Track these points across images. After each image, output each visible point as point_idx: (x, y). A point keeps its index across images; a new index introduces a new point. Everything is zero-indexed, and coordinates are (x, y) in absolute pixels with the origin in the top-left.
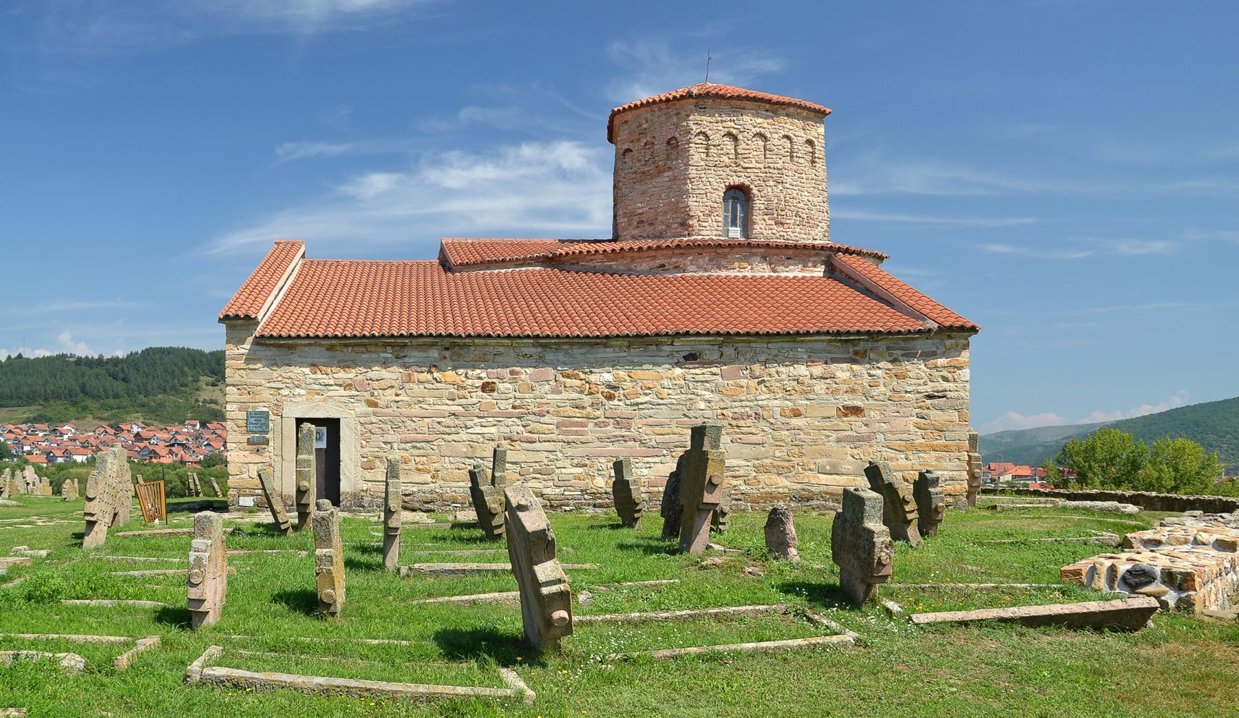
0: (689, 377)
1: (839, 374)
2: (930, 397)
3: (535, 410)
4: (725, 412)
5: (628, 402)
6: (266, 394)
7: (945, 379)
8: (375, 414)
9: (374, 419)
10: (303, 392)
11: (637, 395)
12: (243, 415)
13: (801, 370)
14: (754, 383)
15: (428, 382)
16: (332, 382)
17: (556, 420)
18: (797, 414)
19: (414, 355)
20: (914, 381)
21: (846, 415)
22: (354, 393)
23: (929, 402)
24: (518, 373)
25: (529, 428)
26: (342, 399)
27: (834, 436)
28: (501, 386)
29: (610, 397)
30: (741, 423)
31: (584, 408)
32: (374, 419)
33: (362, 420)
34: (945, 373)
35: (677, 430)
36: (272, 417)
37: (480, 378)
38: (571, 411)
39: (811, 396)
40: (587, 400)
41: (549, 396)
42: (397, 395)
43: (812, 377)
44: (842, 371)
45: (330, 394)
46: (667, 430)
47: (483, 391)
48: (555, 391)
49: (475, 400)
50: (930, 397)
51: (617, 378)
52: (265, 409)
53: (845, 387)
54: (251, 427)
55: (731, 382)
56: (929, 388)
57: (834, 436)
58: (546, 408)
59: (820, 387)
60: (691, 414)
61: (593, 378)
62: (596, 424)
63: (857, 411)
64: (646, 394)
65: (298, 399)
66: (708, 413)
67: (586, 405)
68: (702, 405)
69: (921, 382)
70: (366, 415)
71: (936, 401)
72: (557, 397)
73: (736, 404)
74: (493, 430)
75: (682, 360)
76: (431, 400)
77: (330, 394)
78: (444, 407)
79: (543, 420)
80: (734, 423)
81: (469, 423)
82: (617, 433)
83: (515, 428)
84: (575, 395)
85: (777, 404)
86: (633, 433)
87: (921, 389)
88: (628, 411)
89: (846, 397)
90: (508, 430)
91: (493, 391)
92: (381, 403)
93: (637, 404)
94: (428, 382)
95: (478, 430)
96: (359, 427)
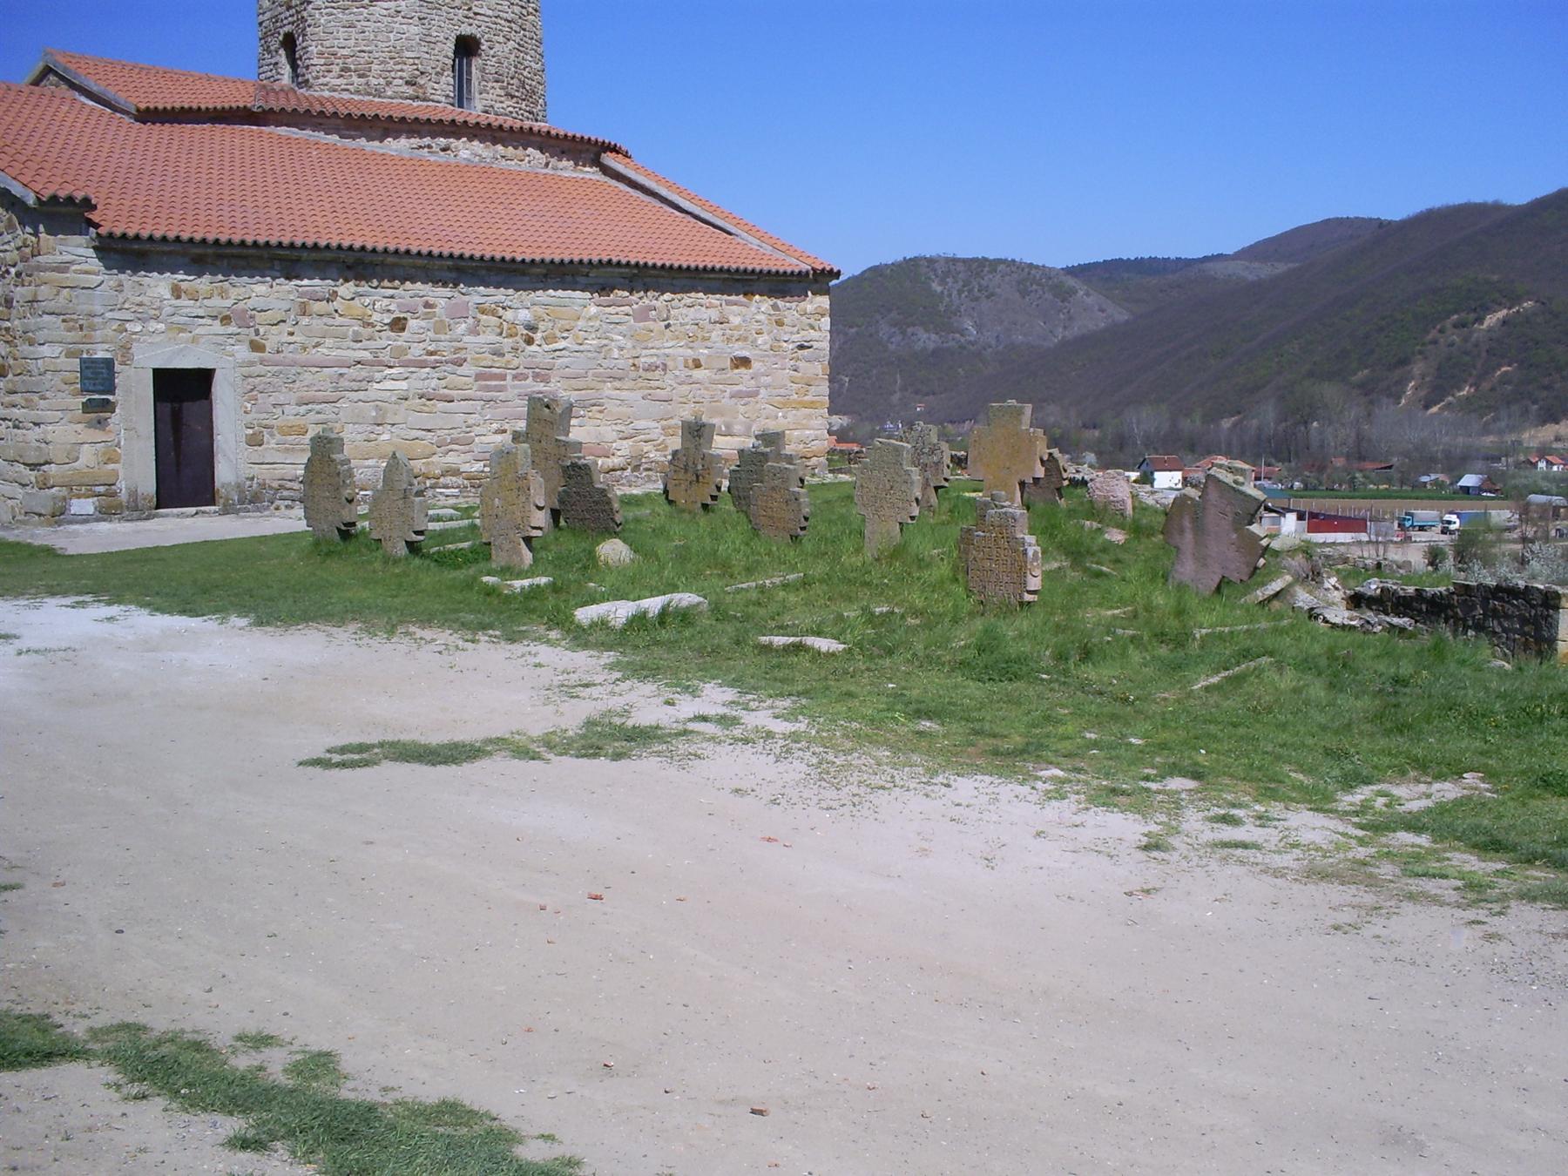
1: (731, 318)
5: (546, 348)
9: (260, 369)
10: (161, 326)
11: (554, 339)
12: (75, 363)
15: (329, 315)
18: (697, 365)
26: (220, 339)
29: (530, 341)
30: (649, 375)
32: (260, 369)
33: (245, 371)
34: (812, 321)
38: (489, 359)
41: (466, 339)
42: (292, 334)
45: (199, 331)
46: (580, 383)
48: (474, 331)
49: (384, 343)
50: (801, 347)
52: (108, 356)
57: (729, 389)
58: (461, 355)
59: (716, 334)
60: (605, 363)
62: (515, 377)
63: (744, 362)
65: (158, 339)
68: (616, 353)
70: (251, 364)
71: (806, 352)
74: (404, 385)
77: (199, 331)
79: (460, 370)
81: (378, 376)
90: (420, 384)
91: (403, 329)
94: (329, 315)
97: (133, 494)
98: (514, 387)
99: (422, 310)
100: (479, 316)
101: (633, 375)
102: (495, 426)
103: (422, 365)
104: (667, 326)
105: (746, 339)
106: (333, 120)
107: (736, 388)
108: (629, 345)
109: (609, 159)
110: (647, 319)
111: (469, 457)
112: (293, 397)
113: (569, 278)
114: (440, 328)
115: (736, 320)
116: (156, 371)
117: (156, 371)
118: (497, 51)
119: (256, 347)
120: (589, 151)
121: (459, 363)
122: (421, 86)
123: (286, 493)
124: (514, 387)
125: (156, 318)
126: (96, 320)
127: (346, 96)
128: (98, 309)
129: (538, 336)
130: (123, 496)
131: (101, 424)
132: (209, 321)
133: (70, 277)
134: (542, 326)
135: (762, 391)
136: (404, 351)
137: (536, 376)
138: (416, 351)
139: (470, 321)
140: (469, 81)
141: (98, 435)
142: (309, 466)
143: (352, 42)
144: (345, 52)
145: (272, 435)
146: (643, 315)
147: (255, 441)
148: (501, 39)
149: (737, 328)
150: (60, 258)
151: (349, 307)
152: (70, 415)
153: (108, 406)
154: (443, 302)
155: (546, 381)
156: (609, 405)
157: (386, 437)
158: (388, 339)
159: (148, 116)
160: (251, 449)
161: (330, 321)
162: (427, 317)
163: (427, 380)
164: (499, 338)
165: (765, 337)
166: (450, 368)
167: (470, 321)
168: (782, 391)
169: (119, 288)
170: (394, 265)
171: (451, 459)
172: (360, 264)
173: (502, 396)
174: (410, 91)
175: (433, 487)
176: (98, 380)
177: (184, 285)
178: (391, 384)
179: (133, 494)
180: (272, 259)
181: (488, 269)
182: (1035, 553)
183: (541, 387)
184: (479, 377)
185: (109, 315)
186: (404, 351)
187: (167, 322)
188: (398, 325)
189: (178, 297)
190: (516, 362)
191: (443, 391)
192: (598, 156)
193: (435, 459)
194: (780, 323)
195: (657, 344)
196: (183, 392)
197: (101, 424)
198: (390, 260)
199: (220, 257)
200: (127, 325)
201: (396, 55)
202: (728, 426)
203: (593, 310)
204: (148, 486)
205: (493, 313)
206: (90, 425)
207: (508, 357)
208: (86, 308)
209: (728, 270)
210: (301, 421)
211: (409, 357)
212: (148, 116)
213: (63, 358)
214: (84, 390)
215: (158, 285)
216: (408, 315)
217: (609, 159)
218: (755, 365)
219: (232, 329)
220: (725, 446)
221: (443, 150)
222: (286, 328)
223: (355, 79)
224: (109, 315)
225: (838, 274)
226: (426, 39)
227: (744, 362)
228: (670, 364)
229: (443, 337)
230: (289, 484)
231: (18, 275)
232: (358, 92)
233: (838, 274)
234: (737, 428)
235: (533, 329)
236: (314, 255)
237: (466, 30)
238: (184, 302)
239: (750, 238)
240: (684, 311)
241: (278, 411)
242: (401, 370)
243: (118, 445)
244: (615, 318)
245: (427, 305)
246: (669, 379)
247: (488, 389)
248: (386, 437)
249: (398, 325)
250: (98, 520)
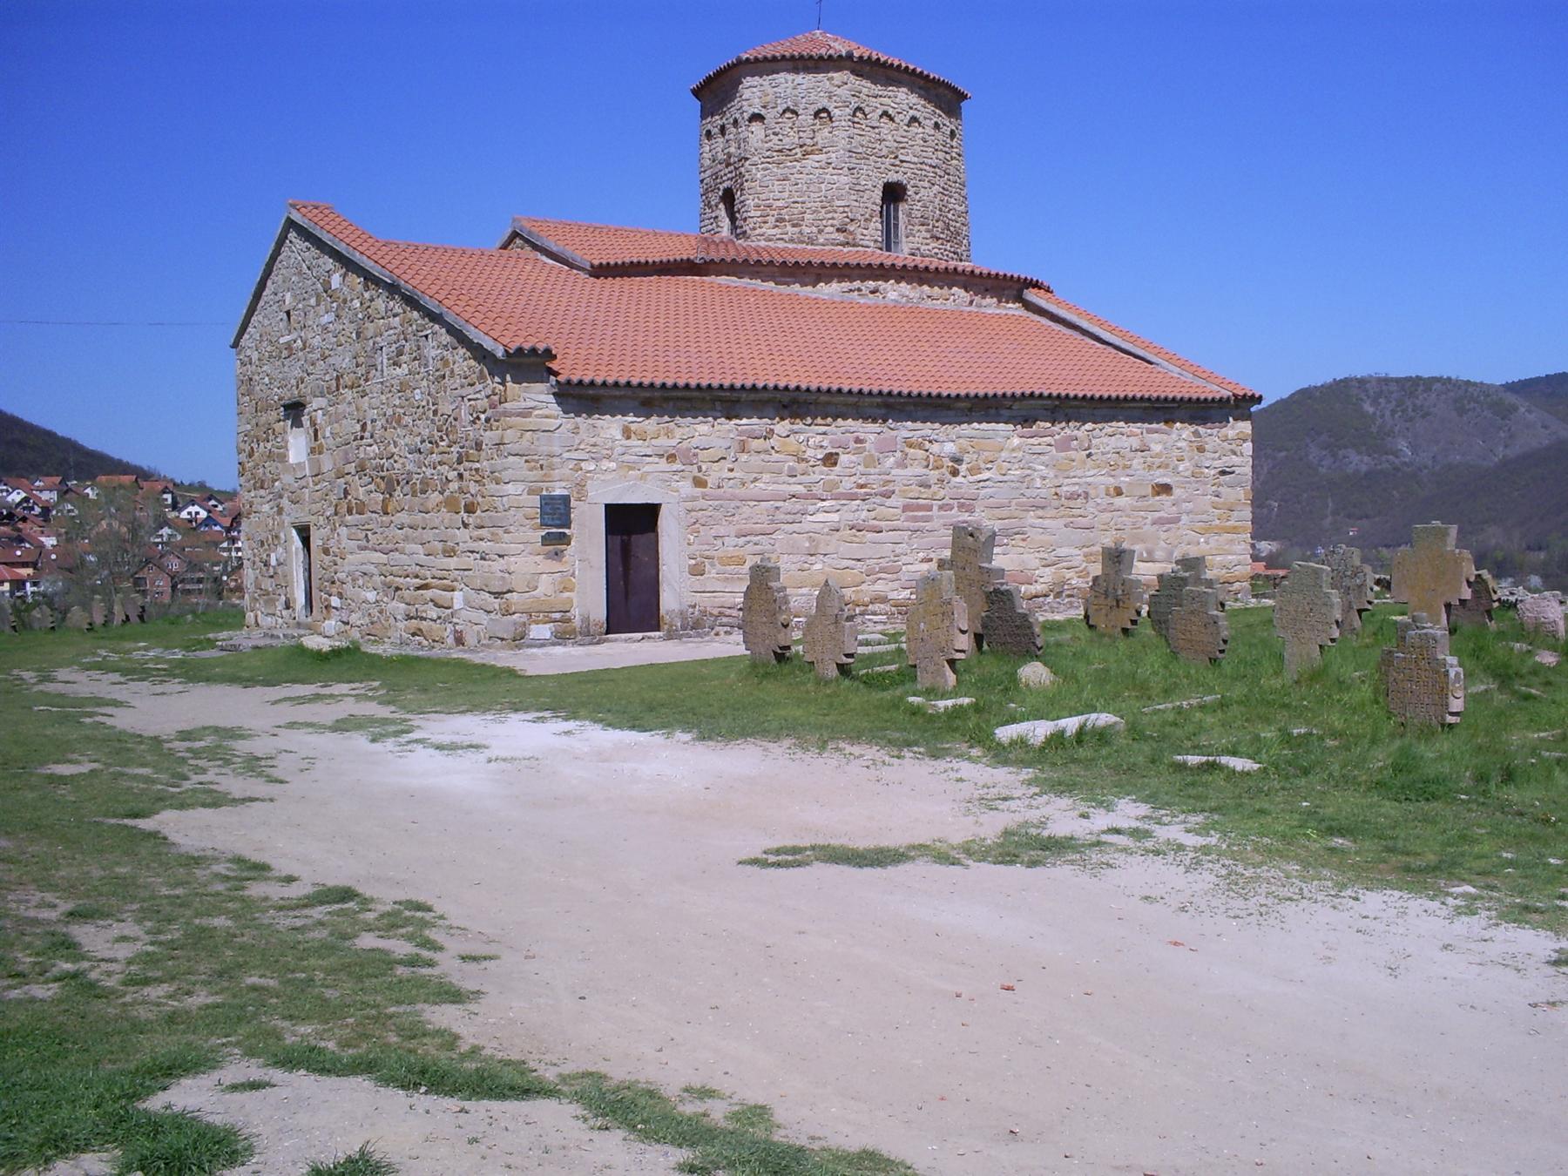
5: (971, 478)
9: (702, 503)
10: (613, 465)
11: (979, 470)
15: (766, 452)
18: (1119, 492)
19: (571, 400)
29: (955, 473)
30: (1071, 503)
32: (702, 503)
33: (689, 505)
34: (1233, 447)
35: (1016, 513)
38: (915, 490)
41: (894, 472)
42: (731, 470)
45: (647, 468)
46: (1004, 513)
48: (901, 464)
49: (817, 477)
50: (1223, 473)
52: (566, 493)
53: (1157, 461)
57: (1151, 516)
58: (890, 487)
59: (1137, 462)
60: (1028, 492)
62: (941, 508)
63: (1165, 489)
65: (609, 477)
68: (1038, 483)
70: (694, 499)
71: (1227, 477)
74: (835, 517)
77: (647, 468)
79: (888, 502)
81: (811, 509)
89: (1158, 472)
90: (851, 516)
91: (835, 464)
94: (766, 452)
97: (586, 620)
99: (852, 445)
100: (907, 450)
101: (1056, 503)
102: (921, 555)
103: (853, 497)
104: (1089, 455)
105: (1167, 466)
106: (770, 268)
107: (1157, 515)
108: (1052, 475)
109: (1031, 295)
110: (1068, 449)
111: (896, 585)
112: (733, 530)
113: (993, 411)
114: (871, 462)
115: (1157, 448)
116: (607, 506)
117: (607, 506)
118: (922, 197)
119: (699, 483)
120: (1012, 288)
121: (888, 495)
122: (851, 233)
123: (725, 620)
125: (608, 457)
126: (555, 460)
127: (781, 245)
128: (556, 450)
129: (963, 468)
130: (577, 623)
131: (557, 555)
133: (531, 422)
134: (966, 458)
135: (1184, 517)
136: (836, 485)
137: (961, 506)
138: (847, 485)
139: (898, 454)
140: (896, 226)
141: (554, 566)
142: (748, 594)
143: (786, 195)
144: (780, 204)
145: (713, 565)
146: (1064, 446)
147: (697, 571)
148: (926, 184)
149: (1158, 455)
150: (523, 405)
151: (785, 444)
152: (530, 547)
153: (564, 539)
154: (872, 437)
155: (971, 511)
156: (1031, 533)
157: (818, 566)
158: (821, 474)
159: (601, 271)
162: (858, 452)
163: (858, 512)
164: (925, 471)
165: (1187, 464)
166: (878, 500)
167: (898, 454)
168: (1204, 517)
169: (576, 430)
170: (828, 403)
171: (880, 587)
172: (794, 403)
173: (928, 526)
174: (841, 237)
175: (862, 614)
176: (556, 515)
177: (633, 427)
178: (823, 516)
179: (586, 620)
181: (915, 405)
182: (1457, 674)
183: (965, 517)
184: (906, 508)
185: (566, 455)
186: (836, 485)
187: (618, 461)
188: (830, 460)
189: (628, 438)
190: (942, 493)
192: (1020, 292)
193: (864, 587)
194: (1201, 450)
195: (1079, 473)
196: (632, 525)
197: (557, 555)
198: (823, 398)
199: (667, 399)
200: (582, 464)
201: (827, 204)
202: (1150, 553)
203: (1016, 441)
204: (600, 613)
205: (920, 446)
206: (548, 556)
207: (935, 488)
208: (544, 449)
209: (1149, 399)
210: (740, 552)
211: (841, 490)
212: (601, 271)
213: (525, 496)
214: (544, 524)
215: (610, 427)
216: (839, 450)
217: (1031, 295)
218: (1177, 492)
219: (677, 466)
220: (1145, 572)
221: (872, 292)
222: (727, 464)
223: (789, 228)
224: (566, 455)
225: (1260, 399)
226: (856, 188)
227: (1165, 489)
228: (1092, 493)
229: (872, 471)
230: (728, 612)
231: (488, 420)
232: (792, 241)
233: (1260, 399)
234: (1159, 554)
235: (958, 460)
236: (752, 396)
237: (893, 177)
238: (634, 442)
239: (1171, 367)
240: (1105, 440)
241: (719, 542)
243: (573, 575)
244: (1038, 449)
245: (858, 441)
246: (1090, 507)
247: (915, 519)
248: (818, 566)
249: (830, 460)
250: (554, 644)
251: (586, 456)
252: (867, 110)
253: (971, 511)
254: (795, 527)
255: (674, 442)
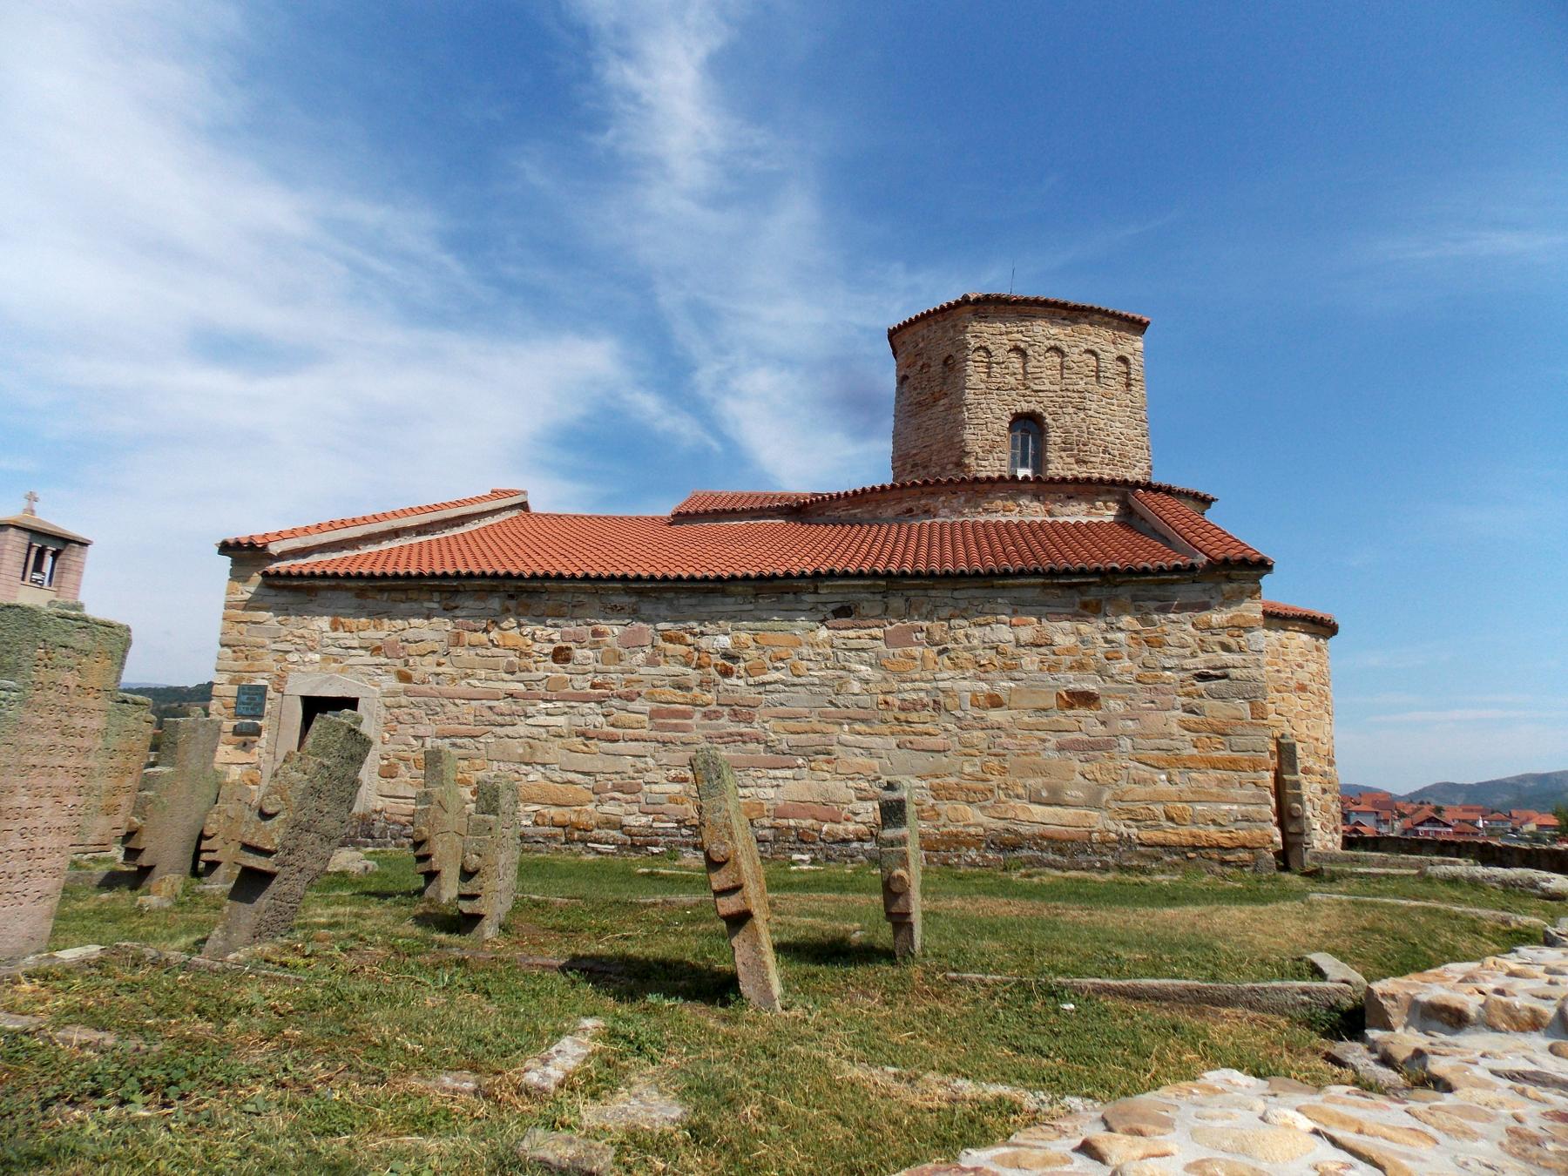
0: (837, 642)
2: (1203, 677)
3: (623, 690)
4: (889, 698)
5: (751, 681)
6: (268, 661)
7: (1226, 648)
8: (406, 692)
9: (404, 700)
10: (317, 657)
11: (763, 669)
13: (1003, 633)
14: (931, 652)
15: (482, 645)
16: (355, 643)
17: (648, 706)
18: (995, 702)
20: (1175, 651)
21: (1071, 707)
22: (383, 660)
23: (1201, 685)
24: (602, 634)
25: (611, 719)
27: (1053, 740)
28: (578, 654)
29: (726, 673)
30: (913, 716)
31: (689, 689)
32: (404, 700)
33: (388, 701)
34: (1225, 638)
35: (819, 727)
36: (271, 694)
37: (551, 641)
39: (1016, 675)
40: (693, 675)
41: (642, 670)
42: (439, 665)
43: (1018, 644)
44: (1063, 633)
46: (804, 726)
47: (555, 661)
48: (652, 662)
49: (541, 674)
50: (1203, 677)
51: (736, 643)
52: (265, 683)
54: (242, 709)
55: (898, 651)
56: (1200, 663)
57: (1053, 740)
58: (636, 688)
59: (1030, 660)
60: (840, 700)
61: (703, 643)
62: (705, 715)
63: (1087, 699)
64: (776, 669)
65: (310, 668)
66: (865, 700)
67: (693, 684)
68: (856, 687)
69: (1188, 652)
70: (394, 694)
71: (1213, 684)
72: (653, 671)
73: (908, 686)
74: (561, 720)
75: (829, 615)
76: (483, 673)
78: (499, 685)
79: (631, 706)
80: (902, 716)
81: (531, 710)
82: (733, 728)
83: (590, 719)
84: (678, 669)
85: (967, 685)
86: (756, 728)
87: (1189, 663)
88: (751, 694)
89: (1071, 675)
90: (581, 721)
91: (567, 660)
92: (416, 676)
93: (764, 684)
94: (482, 645)
95: (542, 720)
96: (383, 712)
98: (704, 727)
102: (673, 773)
103: (586, 699)
119: (405, 677)
124: (704, 727)
132: (362, 652)
138: (582, 684)
139: (648, 650)
141: (242, 756)
145: (408, 767)
148: (1071, 410)
155: (749, 721)
158: (549, 669)
160: (383, 781)
161: (484, 652)
162: (595, 646)
163: (592, 716)
166: (616, 702)
168: (1164, 743)
171: (609, 808)
178: (548, 717)
180: (432, 589)
184: (653, 715)
186: (564, 683)
189: (336, 630)
191: (608, 729)
193: (590, 807)
197: (245, 746)
199: (381, 590)
211: (570, 690)
214: (236, 715)
216: (571, 645)
227: (1087, 699)
234: (1072, 794)
235: (734, 658)
237: (1023, 407)
242: (559, 704)
244: (854, 644)
251: (292, 648)
252: (991, 347)
253: (749, 721)
254: (509, 730)
255: (382, 634)
